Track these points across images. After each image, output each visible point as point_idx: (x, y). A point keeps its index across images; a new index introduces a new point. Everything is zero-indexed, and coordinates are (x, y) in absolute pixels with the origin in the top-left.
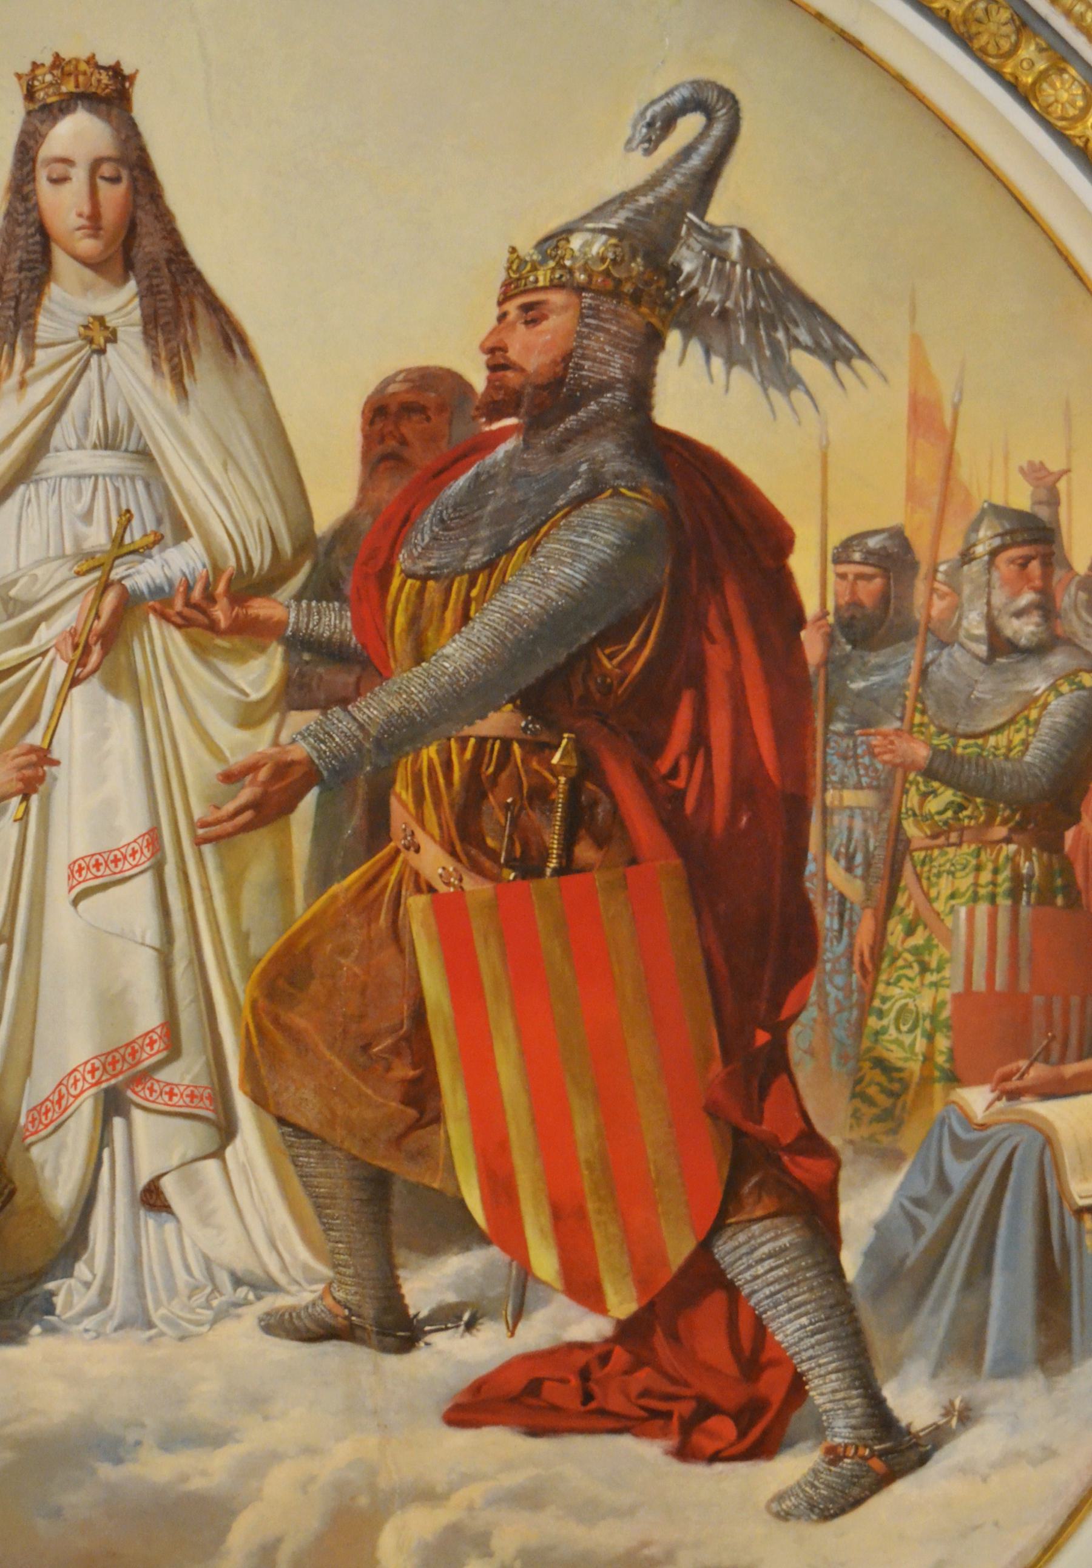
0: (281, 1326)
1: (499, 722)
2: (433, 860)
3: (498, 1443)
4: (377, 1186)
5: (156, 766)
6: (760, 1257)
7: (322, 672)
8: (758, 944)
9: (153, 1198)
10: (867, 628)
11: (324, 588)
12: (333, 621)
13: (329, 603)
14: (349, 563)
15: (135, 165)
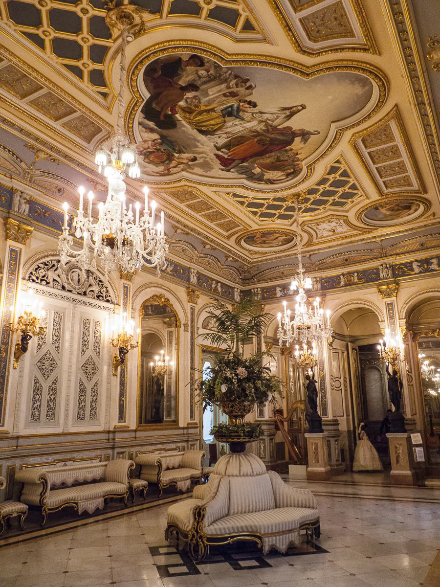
0: (215, 146)
1: (268, 139)
2: (256, 140)
3: (214, 156)
4: (229, 145)
5: (254, 126)
6: (236, 162)
7: (267, 131)
8: (260, 154)
9: (219, 137)
10: (286, 151)
11: (273, 129)
12: (271, 130)
13: (271, 128)
14: (275, 128)
15: (299, 111)
